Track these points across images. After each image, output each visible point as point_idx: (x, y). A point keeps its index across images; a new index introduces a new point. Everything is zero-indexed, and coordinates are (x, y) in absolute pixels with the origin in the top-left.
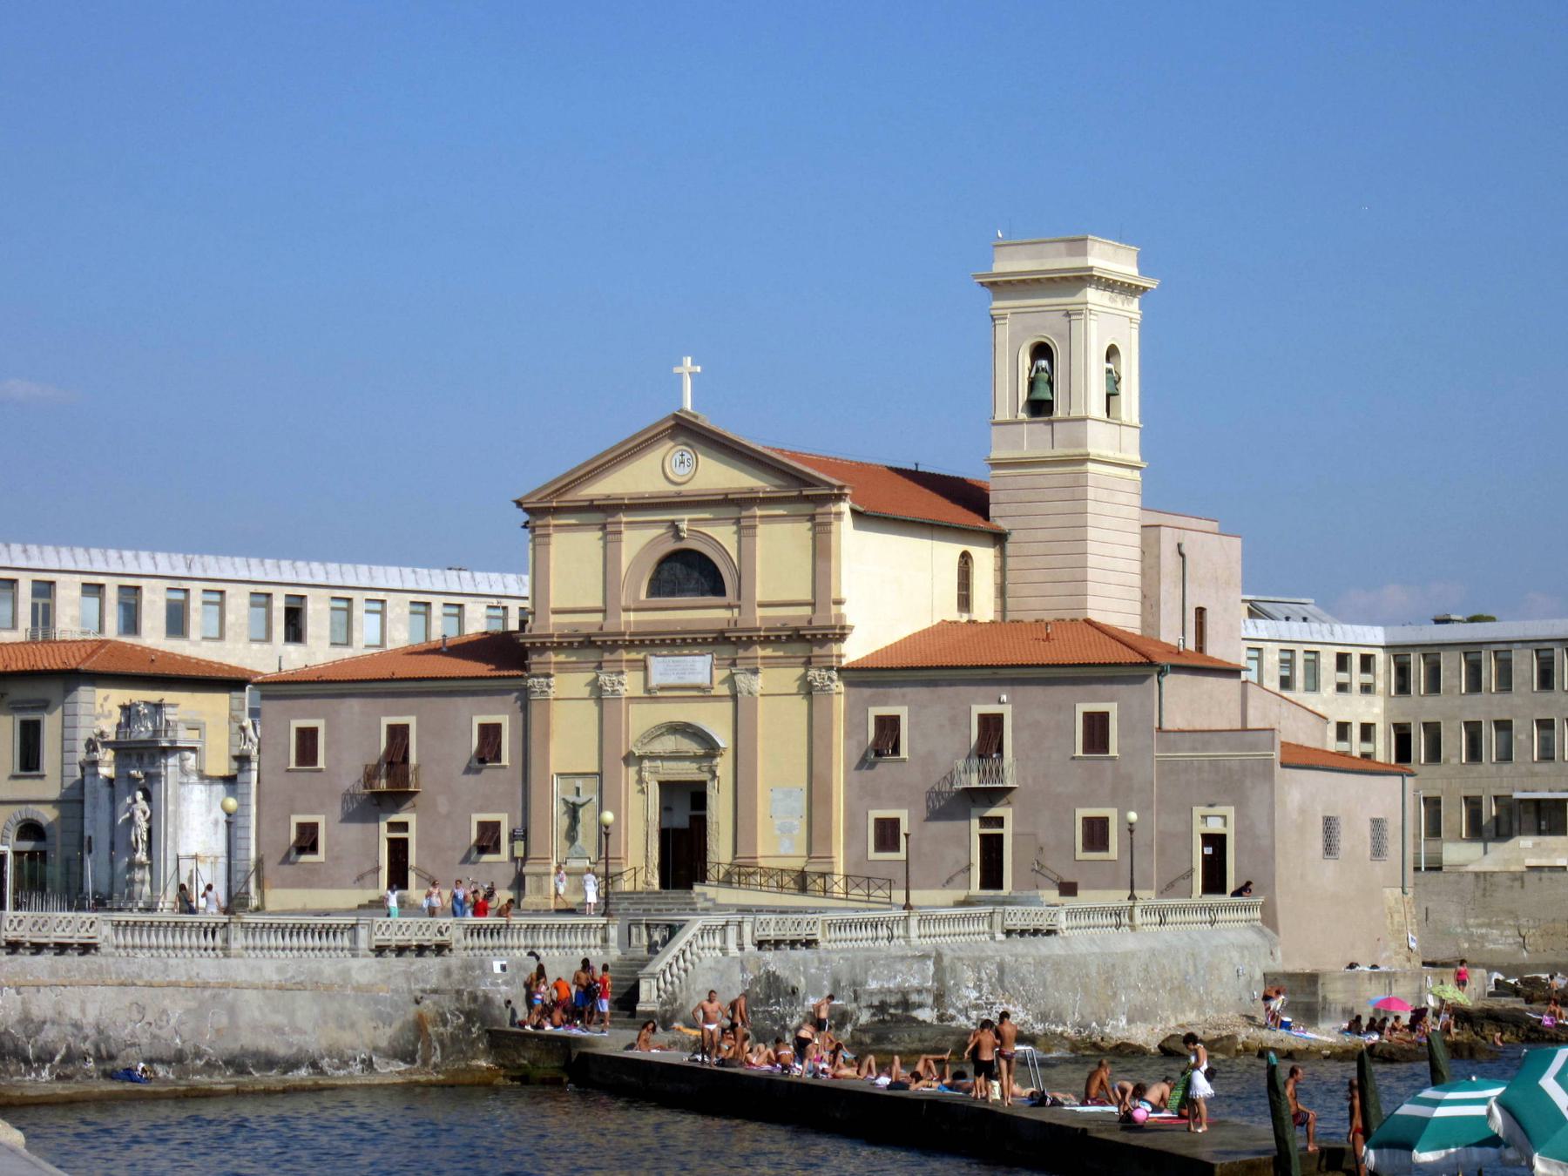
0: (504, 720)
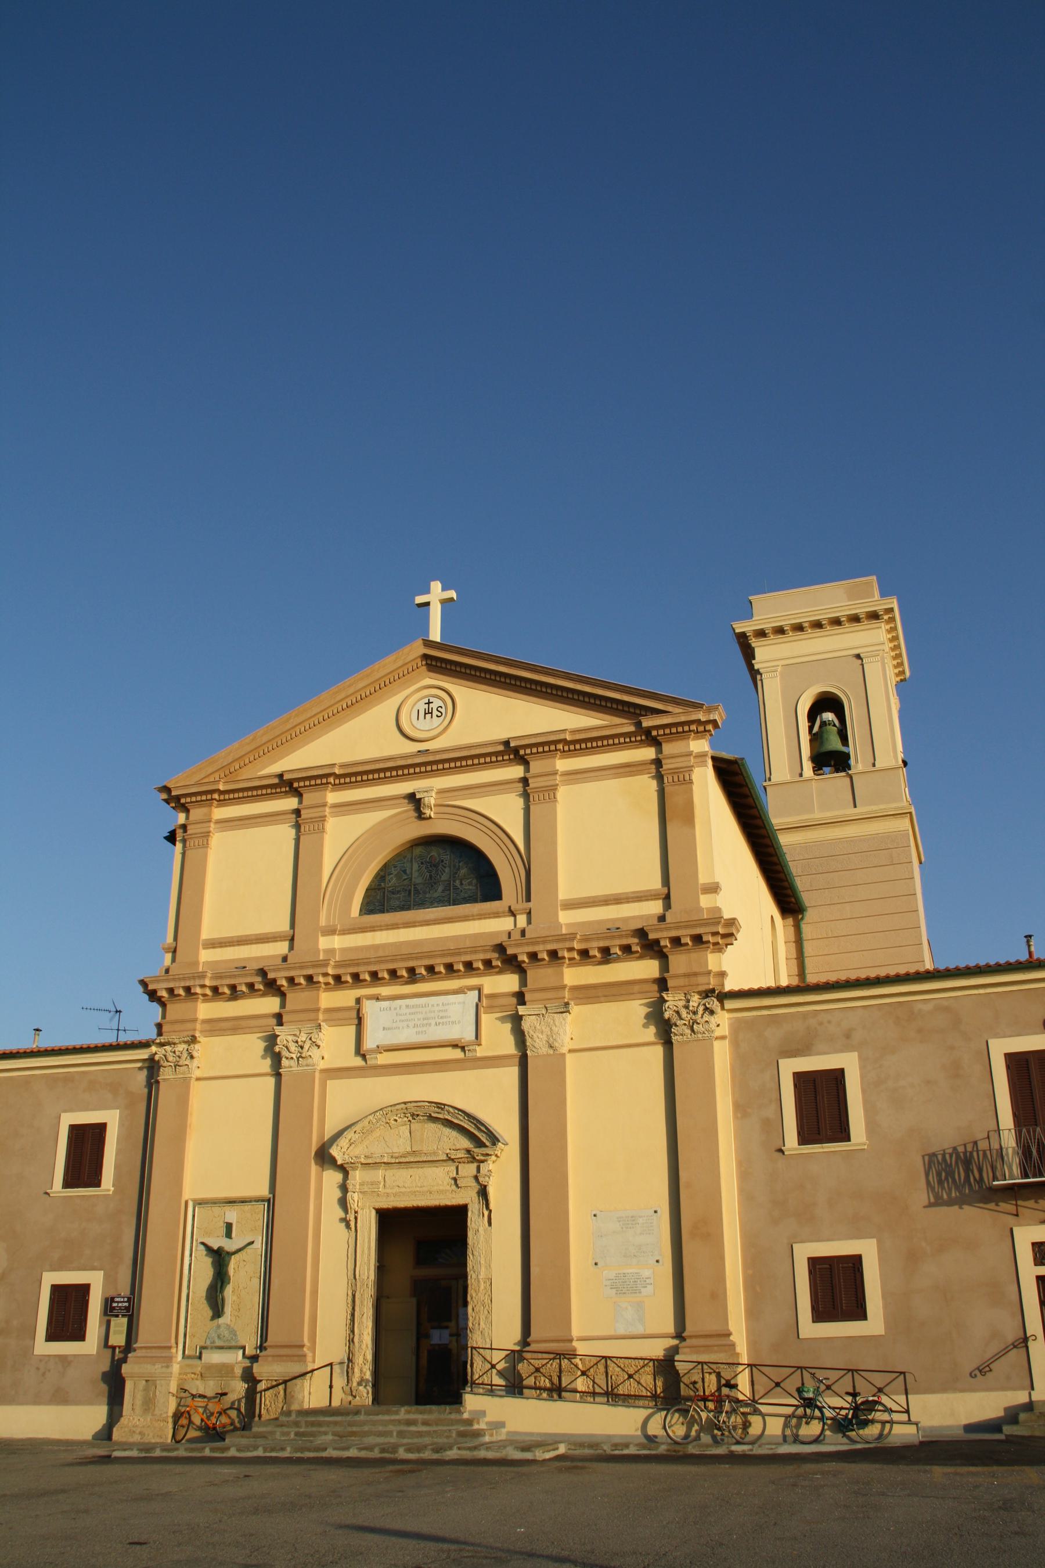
0: (111, 1118)
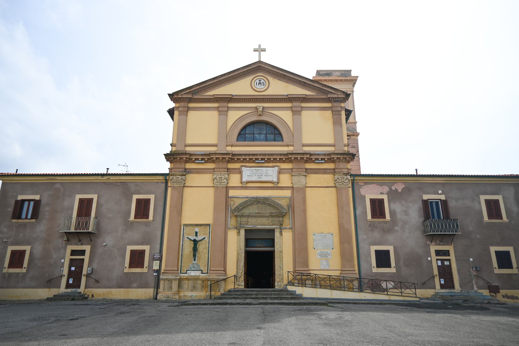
0: (152, 197)
